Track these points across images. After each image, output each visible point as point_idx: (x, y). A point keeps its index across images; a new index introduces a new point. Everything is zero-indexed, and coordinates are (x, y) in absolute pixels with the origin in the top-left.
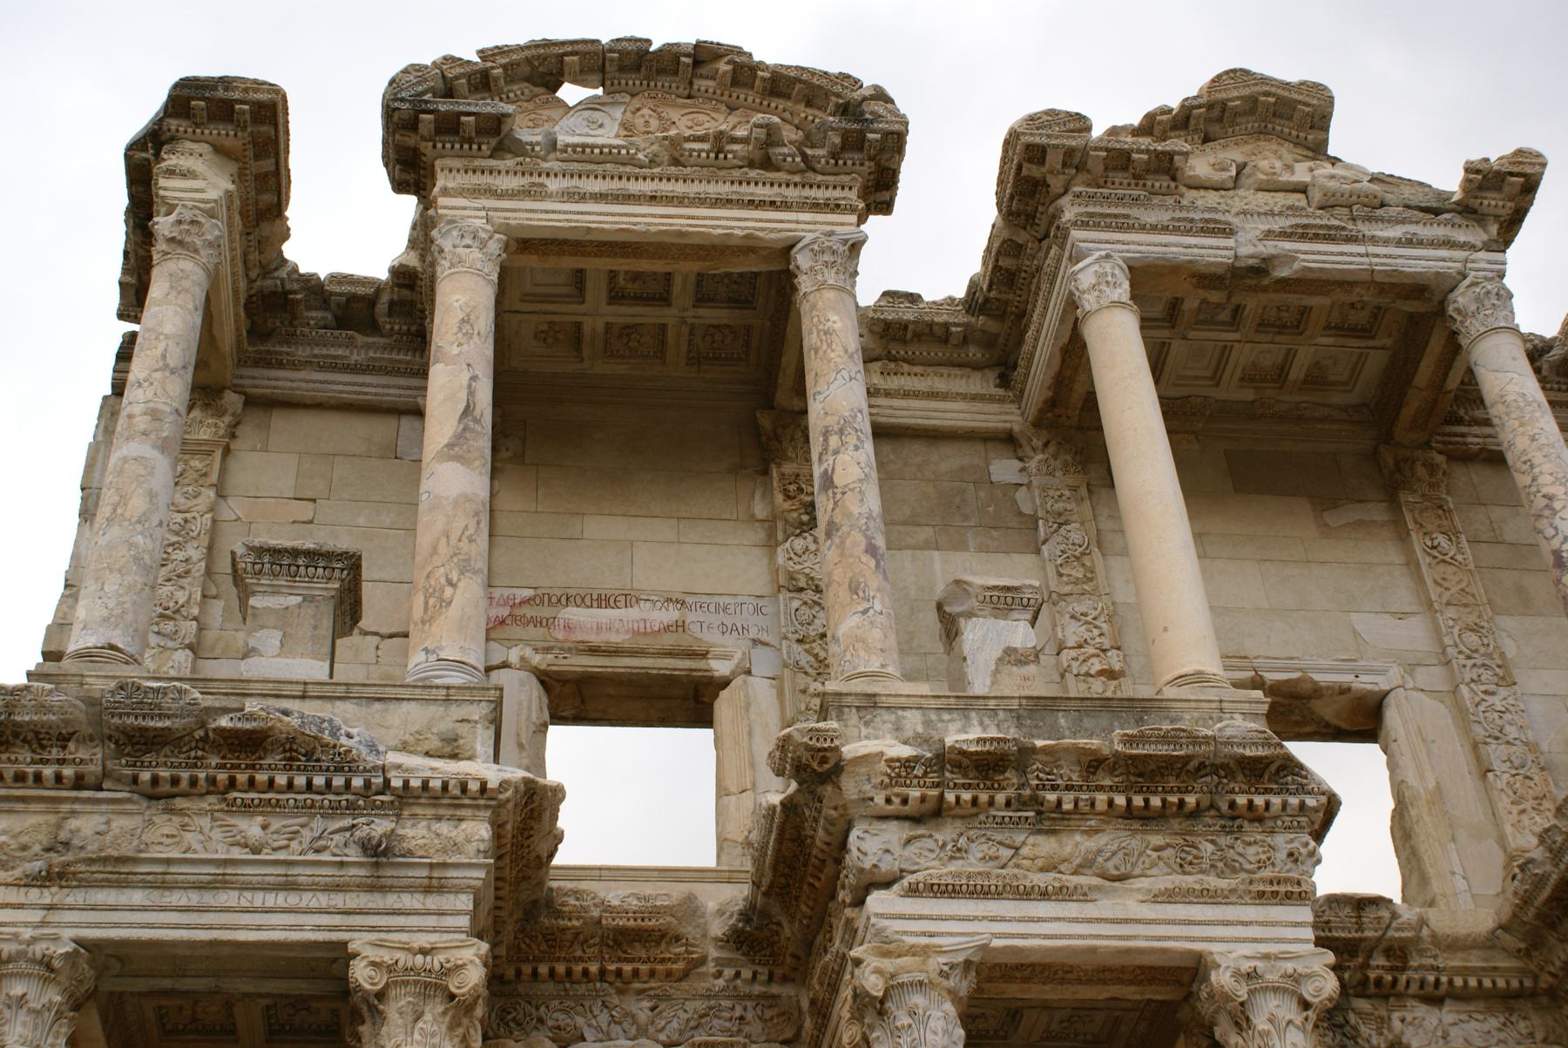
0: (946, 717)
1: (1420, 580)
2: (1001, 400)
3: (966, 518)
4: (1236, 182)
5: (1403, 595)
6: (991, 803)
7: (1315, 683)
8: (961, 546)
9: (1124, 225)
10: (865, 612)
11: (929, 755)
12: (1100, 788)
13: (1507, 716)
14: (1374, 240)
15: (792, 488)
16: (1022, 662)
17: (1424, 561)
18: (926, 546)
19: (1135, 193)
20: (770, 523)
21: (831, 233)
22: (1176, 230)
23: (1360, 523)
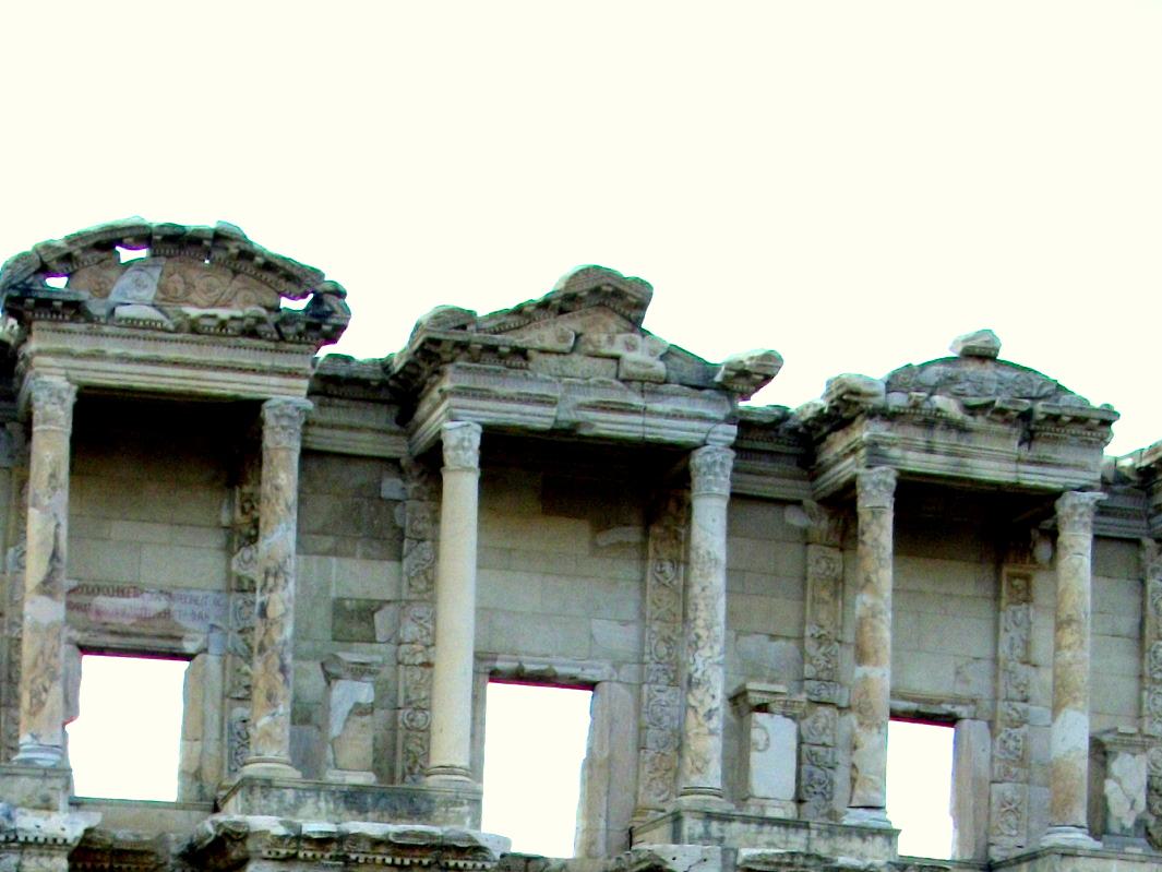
0: (308, 794)
1: (643, 590)
2: (397, 434)
3: (359, 529)
4: (573, 350)
5: (630, 610)
6: (322, 857)
7: (554, 671)
8: (351, 555)
9: (484, 395)
10: (273, 715)
11: (293, 834)
12: (380, 854)
13: (667, 709)
14: (652, 414)
15: (247, 506)
16: (361, 714)
17: (650, 580)
18: (327, 553)
19: (497, 368)
20: (231, 529)
21: (288, 403)
22: (520, 401)
23: (621, 544)
